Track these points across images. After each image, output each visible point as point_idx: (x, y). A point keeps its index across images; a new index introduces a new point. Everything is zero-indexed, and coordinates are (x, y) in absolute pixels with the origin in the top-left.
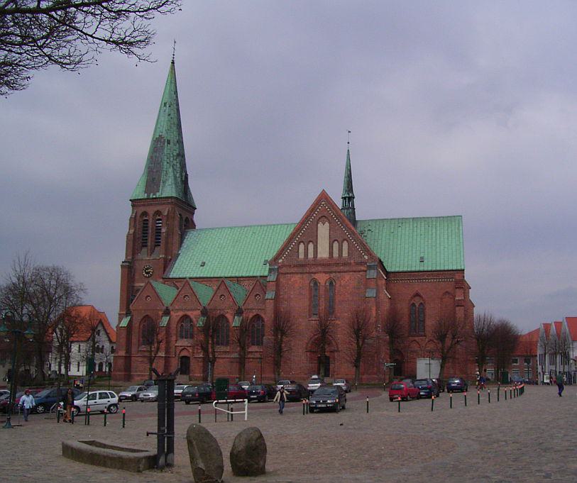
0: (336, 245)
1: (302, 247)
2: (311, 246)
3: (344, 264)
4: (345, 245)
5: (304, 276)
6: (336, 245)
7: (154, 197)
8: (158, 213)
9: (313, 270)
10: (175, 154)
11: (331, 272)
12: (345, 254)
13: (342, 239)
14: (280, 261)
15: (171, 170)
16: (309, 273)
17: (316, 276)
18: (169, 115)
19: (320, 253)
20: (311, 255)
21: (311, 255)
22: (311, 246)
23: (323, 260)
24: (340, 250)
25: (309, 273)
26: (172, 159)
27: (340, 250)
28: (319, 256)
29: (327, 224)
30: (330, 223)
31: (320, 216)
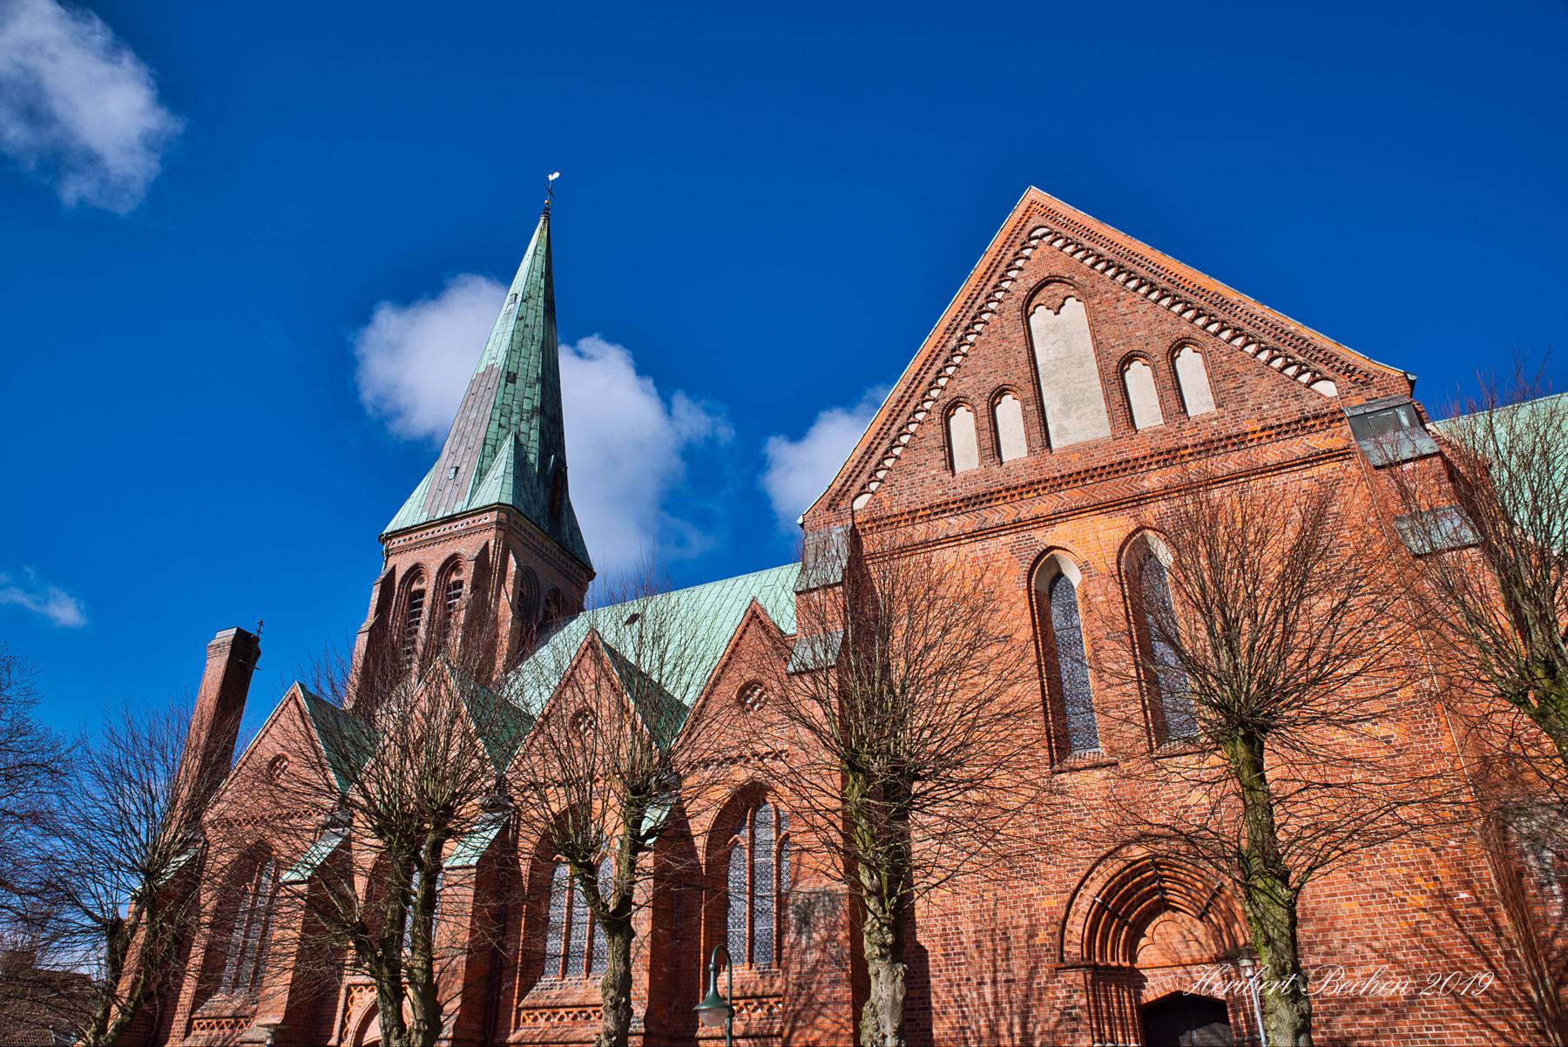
0: (1139, 378)
1: (963, 423)
2: (1010, 412)
3: (1209, 447)
4: (1190, 364)
5: (993, 545)
6: (1139, 378)
7: (448, 514)
8: (452, 564)
9: (1025, 513)
10: (527, 406)
11: (1140, 500)
12: (1199, 397)
13: (1160, 346)
14: (860, 503)
15: (506, 450)
16: (1018, 525)
17: (1056, 535)
18: (520, 318)
19: (1062, 430)
20: (1014, 445)
21: (1014, 445)
22: (1010, 412)
23: (1087, 449)
24: (1172, 389)
25: (1018, 525)
26: (515, 419)
27: (1172, 389)
28: (1055, 444)
29: (1075, 310)
30: (1085, 296)
31: (1032, 282)
